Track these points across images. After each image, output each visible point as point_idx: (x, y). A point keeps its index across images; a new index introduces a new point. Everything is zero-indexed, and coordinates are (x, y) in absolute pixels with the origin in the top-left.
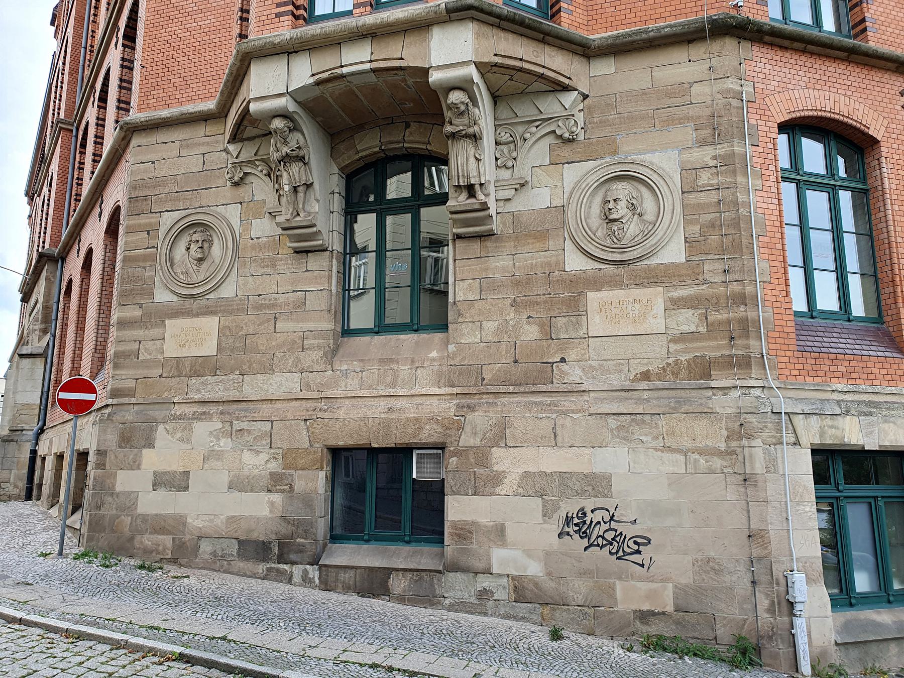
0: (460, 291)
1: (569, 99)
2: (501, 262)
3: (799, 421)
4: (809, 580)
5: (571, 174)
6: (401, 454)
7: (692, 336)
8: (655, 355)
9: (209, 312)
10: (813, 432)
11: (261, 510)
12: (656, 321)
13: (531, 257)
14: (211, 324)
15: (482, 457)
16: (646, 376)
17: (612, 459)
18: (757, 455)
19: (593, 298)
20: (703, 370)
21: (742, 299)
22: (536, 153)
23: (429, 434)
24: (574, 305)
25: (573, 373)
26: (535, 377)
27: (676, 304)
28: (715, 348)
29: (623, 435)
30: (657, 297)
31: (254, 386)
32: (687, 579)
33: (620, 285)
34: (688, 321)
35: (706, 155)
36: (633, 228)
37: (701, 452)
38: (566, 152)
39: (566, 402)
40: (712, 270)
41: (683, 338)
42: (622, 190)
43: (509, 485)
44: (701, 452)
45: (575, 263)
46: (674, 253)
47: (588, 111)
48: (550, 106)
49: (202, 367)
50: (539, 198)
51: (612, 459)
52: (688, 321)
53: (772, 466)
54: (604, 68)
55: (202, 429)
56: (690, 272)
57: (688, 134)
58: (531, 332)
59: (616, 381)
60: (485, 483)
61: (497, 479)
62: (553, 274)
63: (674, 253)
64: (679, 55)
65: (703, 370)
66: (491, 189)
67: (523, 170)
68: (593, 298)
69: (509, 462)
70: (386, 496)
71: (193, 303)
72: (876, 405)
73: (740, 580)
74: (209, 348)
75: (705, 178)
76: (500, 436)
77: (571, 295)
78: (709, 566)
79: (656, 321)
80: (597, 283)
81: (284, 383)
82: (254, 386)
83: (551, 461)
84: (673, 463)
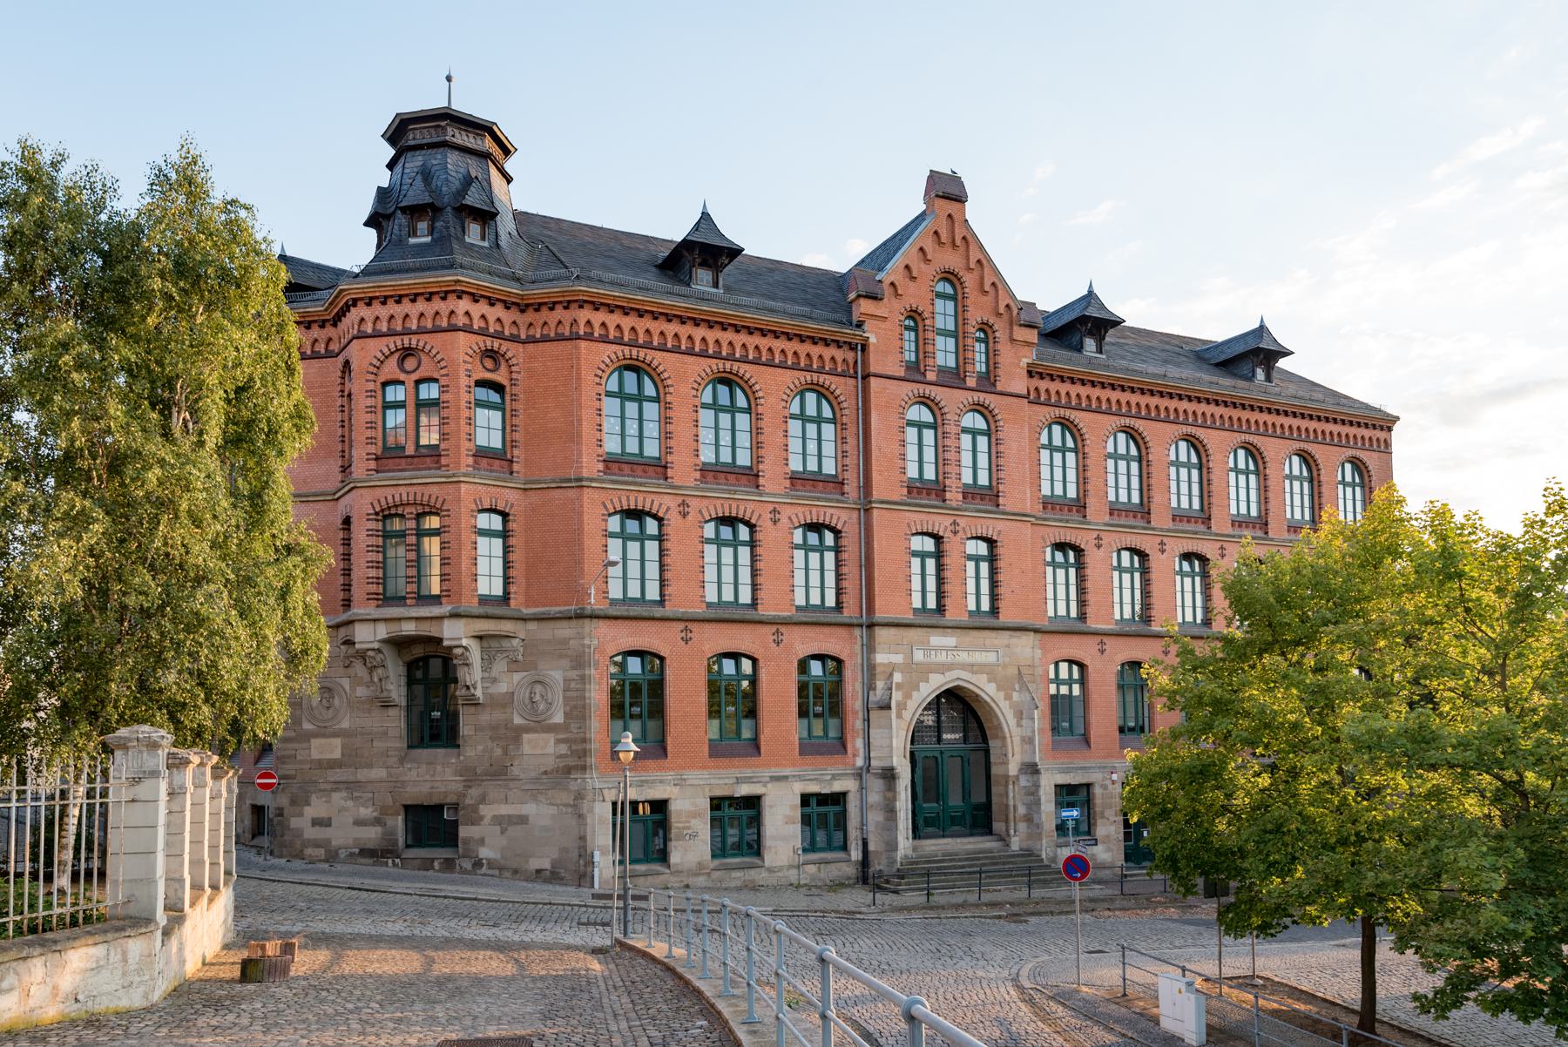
1: (515, 642)
3: (606, 792)
4: (603, 854)
5: (517, 677)
6: (439, 808)
7: (564, 756)
8: (550, 763)
10: (611, 796)
12: (551, 749)
13: (498, 715)
15: (476, 810)
16: (545, 773)
17: (529, 809)
18: (585, 805)
19: (526, 737)
20: (568, 770)
21: (584, 740)
22: (500, 666)
23: (451, 799)
24: (517, 740)
25: (515, 771)
26: (499, 772)
27: (558, 741)
28: (572, 762)
29: (535, 799)
30: (551, 738)
32: (556, 856)
33: (536, 732)
34: (563, 749)
35: (574, 674)
36: (542, 707)
37: (566, 805)
38: (514, 666)
39: (511, 784)
40: (574, 726)
41: (561, 756)
42: (538, 688)
43: (487, 820)
44: (566, 805)
45: (518, 720)
46: (559, 718)
47: (525, 647)
48: (505, 643)
50: (502, 688)
51: (529, 809)
52: (563, 749)
53: (591, 810)
54: (532, 626)
56: (564, 727)
57: (566, 663)
58: (498, 752)
59: (533, 774)
60: (476, 820)
61: (482, 818)
62: (508, 725)
63: (559, 718)
64: (565, 623)
65: (568, 770)
66: (479, 685)
67: (494, 673)
68: (526, 737)
69: (487, 811)
70: (432, 827)
72: (647, 781)
73: (575, 854)
75: (573, 685)
76: (483, 799)
77: (516, 734)
78: (564, 850)
79: (551, 749)
80: (528, 730)
83: (505, 810)
84: (553, 810)
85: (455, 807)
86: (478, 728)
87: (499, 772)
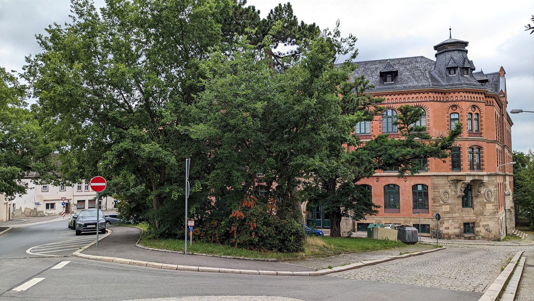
0: (475, 203)
2: (478, 200)
8: (491, 211)
9: (448, 205)
11: (457, 231)
12: (491, 208)
14: (448, 206)
20: (495, 213)
24: (485, 205)
25: (485, 213)
28: (496, 211)
30: (491, 205)
31: (455, 215)
46: (493, 200)
49: (448, 213)
55: (450, 221)
56: (494, 202)
58: (481, 209)
70: (468, 229)
71: (445, 203)
74: (448, 210)
80: (487, 203)
81: (457, 215)
82: (455, 215)
85: (474, 223)
86: (478, 203)
87: (482, 214)
